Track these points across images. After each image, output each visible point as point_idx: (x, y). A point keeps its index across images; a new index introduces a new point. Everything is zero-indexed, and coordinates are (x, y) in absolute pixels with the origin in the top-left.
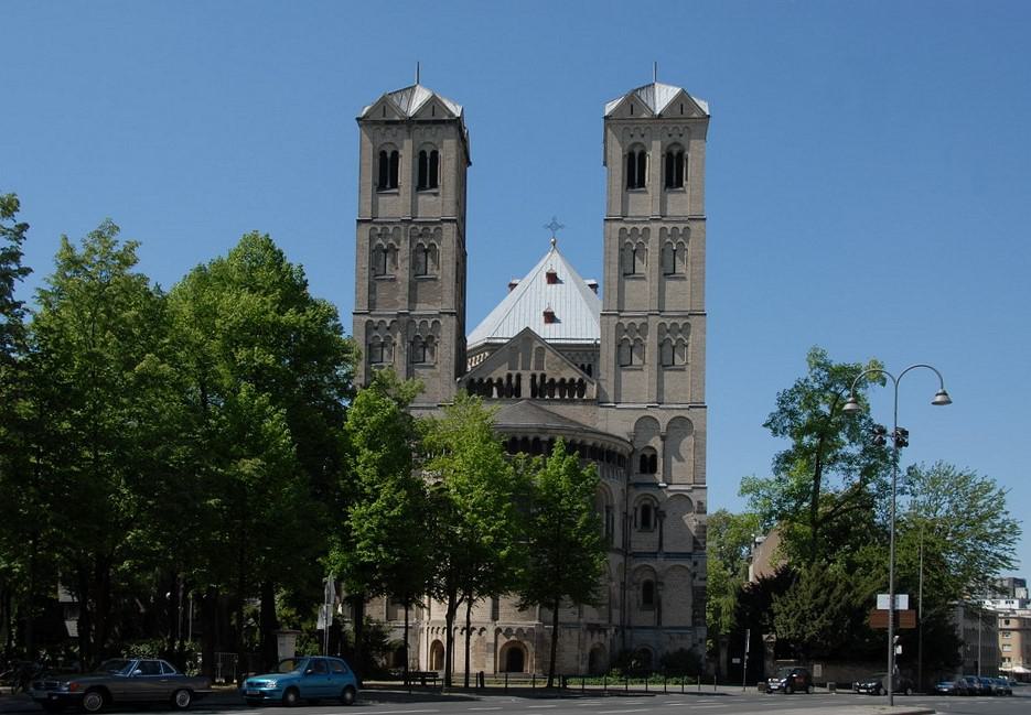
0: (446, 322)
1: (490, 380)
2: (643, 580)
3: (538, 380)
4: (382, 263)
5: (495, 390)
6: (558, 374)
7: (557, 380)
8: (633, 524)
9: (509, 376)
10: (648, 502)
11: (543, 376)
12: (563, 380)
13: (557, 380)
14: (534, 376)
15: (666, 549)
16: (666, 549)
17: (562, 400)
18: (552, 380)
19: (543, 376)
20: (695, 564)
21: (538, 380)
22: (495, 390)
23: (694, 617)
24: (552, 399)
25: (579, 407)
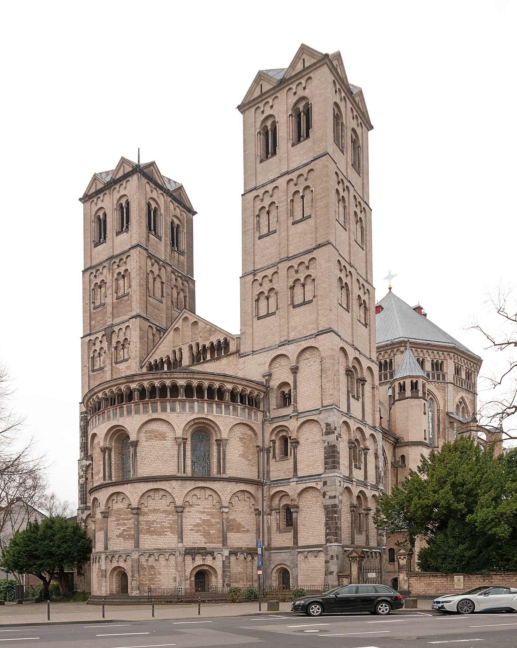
0: (133, 324)
1: (162, 360)
2: (281, 505)
3: (194, 348)
4: (99, 297)
5: (165, 366)
6: (208, 339)
7: (208, 345)
8: (271, 455)
9: (174, 352)
10: (284, 434)
11: (198, 345)
12: (212, 344)
13: (208, 345)
14: (191, 347)
15: (300, 474)
16: (300, 474)
17: (213, 359)
18: (204, 346)
19: (198, 345)
20: (325, 483)
21: (194, 348)
22: (165, 366)
23: (327, 534)
24: (205, 361)
25: (224, 361)
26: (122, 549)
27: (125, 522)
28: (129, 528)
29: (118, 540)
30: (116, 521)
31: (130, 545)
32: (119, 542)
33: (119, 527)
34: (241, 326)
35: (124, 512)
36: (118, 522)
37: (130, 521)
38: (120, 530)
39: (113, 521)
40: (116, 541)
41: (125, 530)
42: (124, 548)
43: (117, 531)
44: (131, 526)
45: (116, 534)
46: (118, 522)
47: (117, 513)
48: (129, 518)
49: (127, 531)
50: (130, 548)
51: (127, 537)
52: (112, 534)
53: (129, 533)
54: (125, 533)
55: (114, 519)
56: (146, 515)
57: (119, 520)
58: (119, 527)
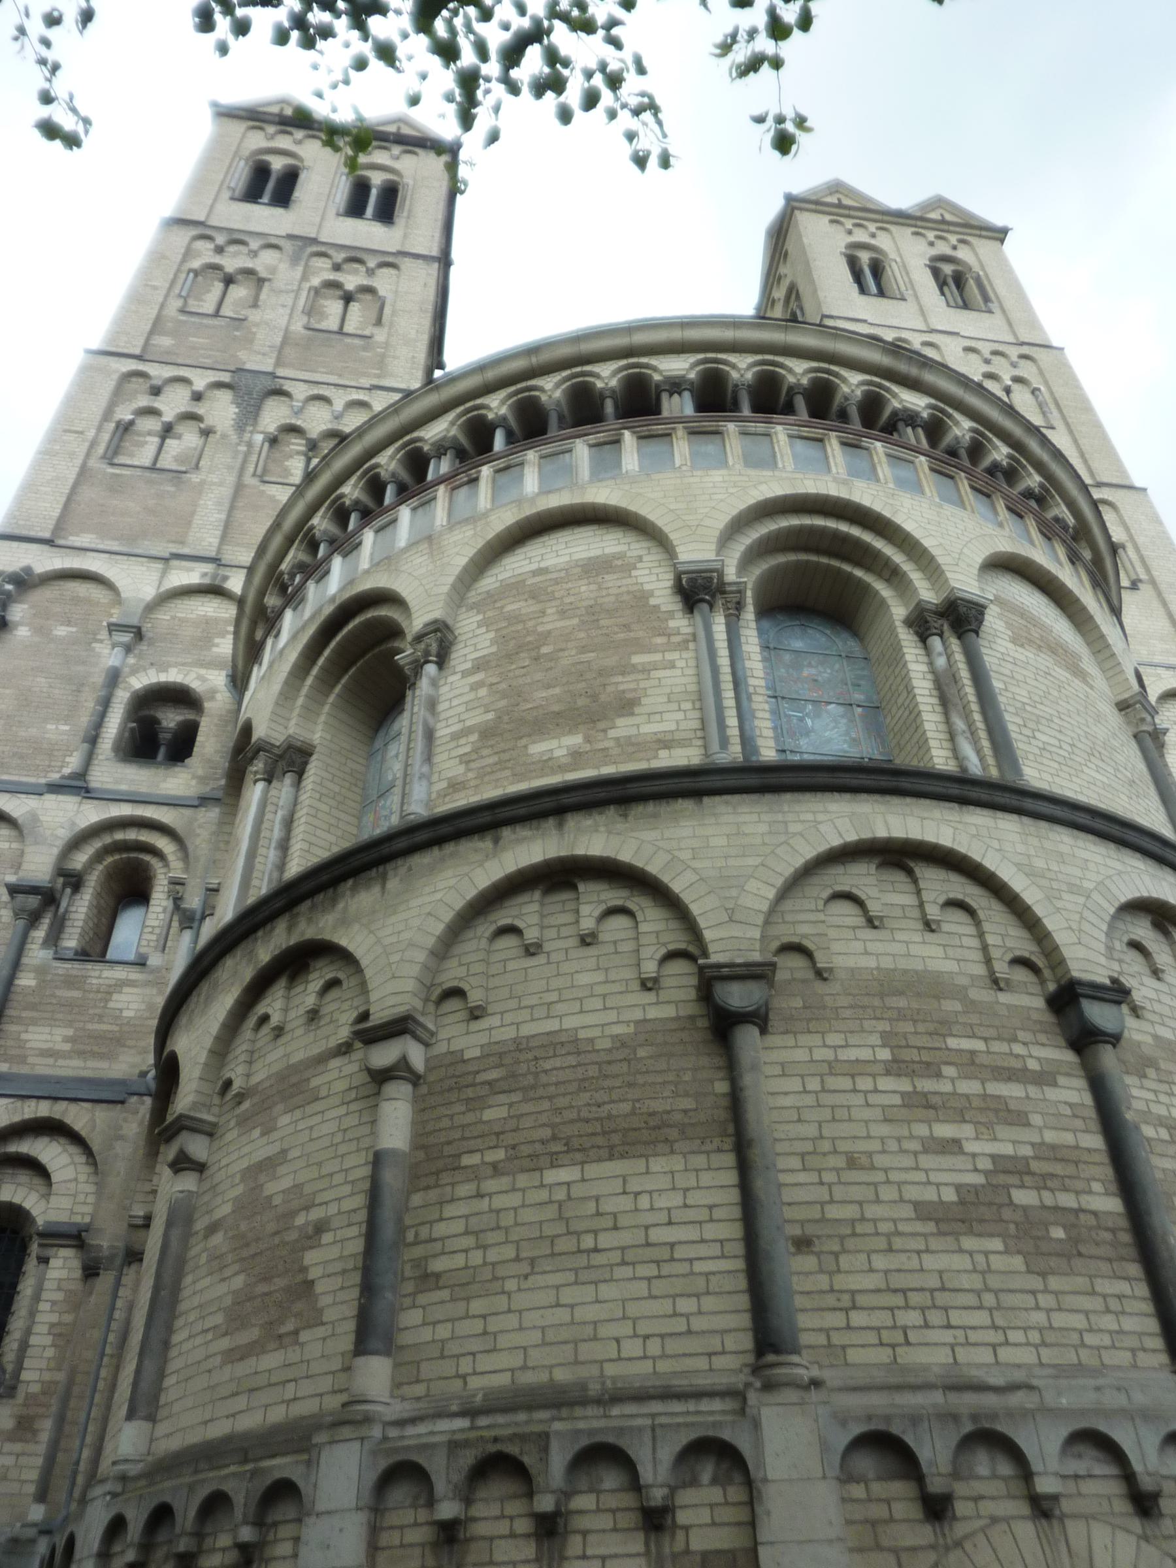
26: (1027, 1356)
27: (997, 1088)
28: (1053, 1152)
29: (963, 1262)
30: (895, 1068)
31: (1108, 1322)
32: (966, 1281)
33: (945, 1131)
34: (1165, 532)
35: (971, 1006)
36: (926, 1085)
37: (1051, 1094)
38: (959, 1162)
39: (855, 1070)
40: (929, 1262)
41: (1004, 1166)
42: (1047, 1355)
43: (926, 1161)
44: (1068, 1138)
45: (912, 1193)
46: (926, 1085)
47: (902, 1003)
48: (1033, 1065)
49: (1043, 1182)
50: (1124, 1358)
51: (1058, 1233)
52: (857, 1193)
53: (1067, 1200)
54: (1023, 1197)
55: (865, 1054)
56: (1151, 1073)
57: (932, 1070)
58: (945, 1131)
